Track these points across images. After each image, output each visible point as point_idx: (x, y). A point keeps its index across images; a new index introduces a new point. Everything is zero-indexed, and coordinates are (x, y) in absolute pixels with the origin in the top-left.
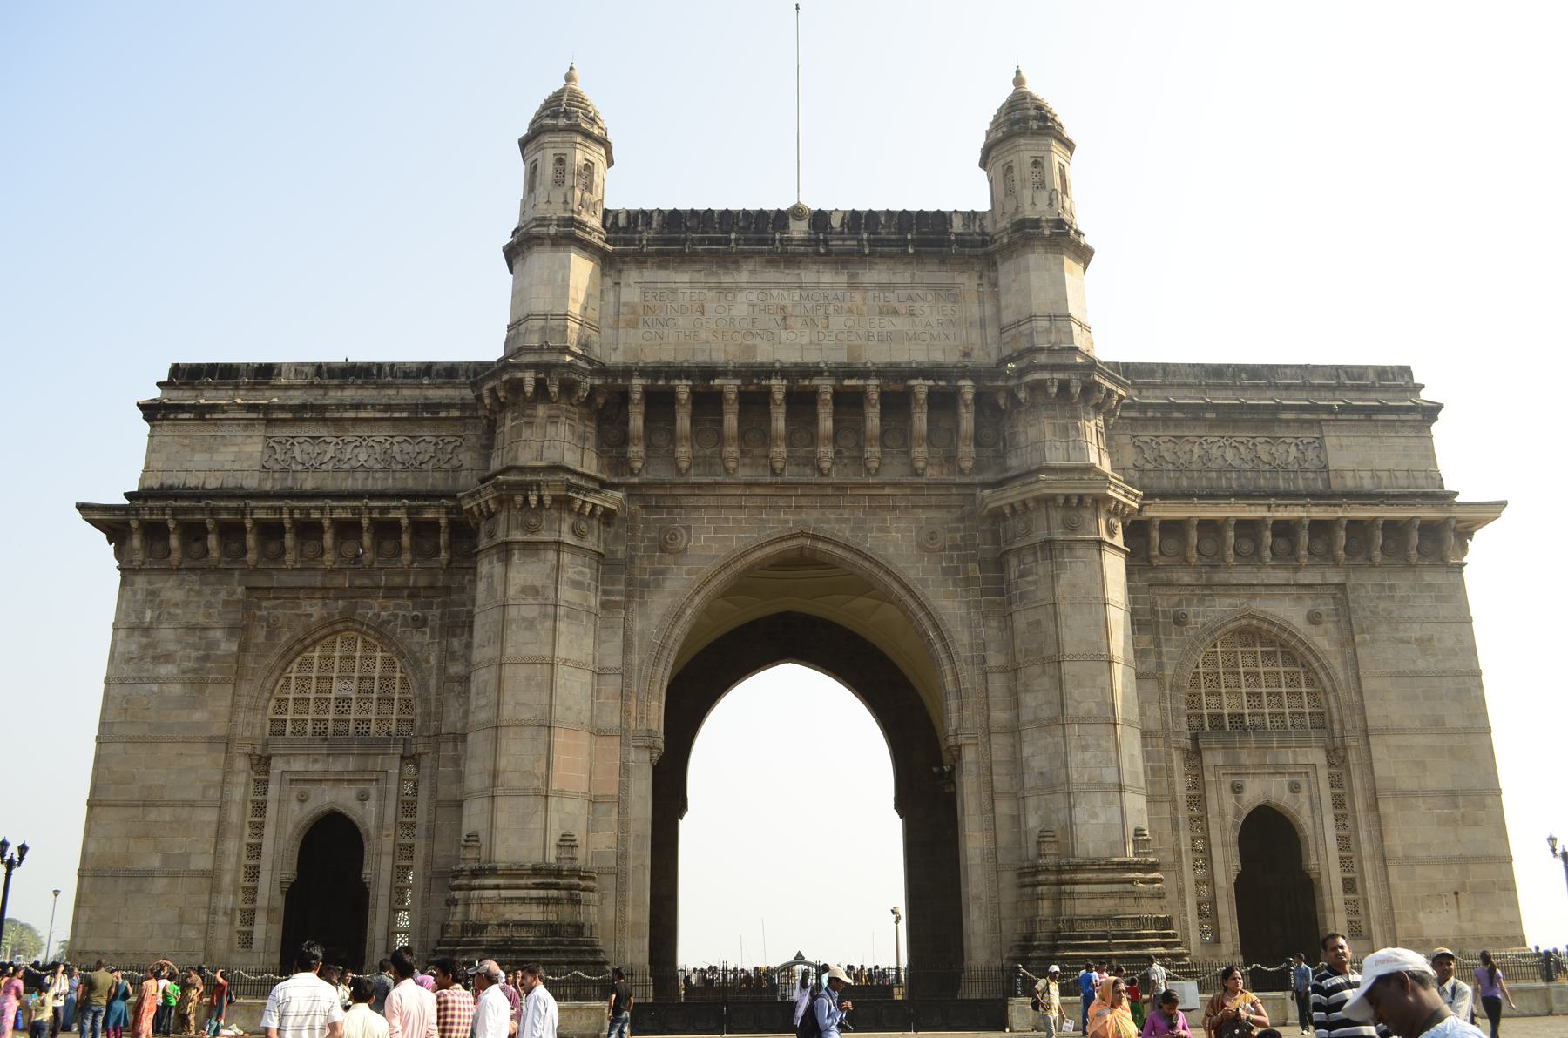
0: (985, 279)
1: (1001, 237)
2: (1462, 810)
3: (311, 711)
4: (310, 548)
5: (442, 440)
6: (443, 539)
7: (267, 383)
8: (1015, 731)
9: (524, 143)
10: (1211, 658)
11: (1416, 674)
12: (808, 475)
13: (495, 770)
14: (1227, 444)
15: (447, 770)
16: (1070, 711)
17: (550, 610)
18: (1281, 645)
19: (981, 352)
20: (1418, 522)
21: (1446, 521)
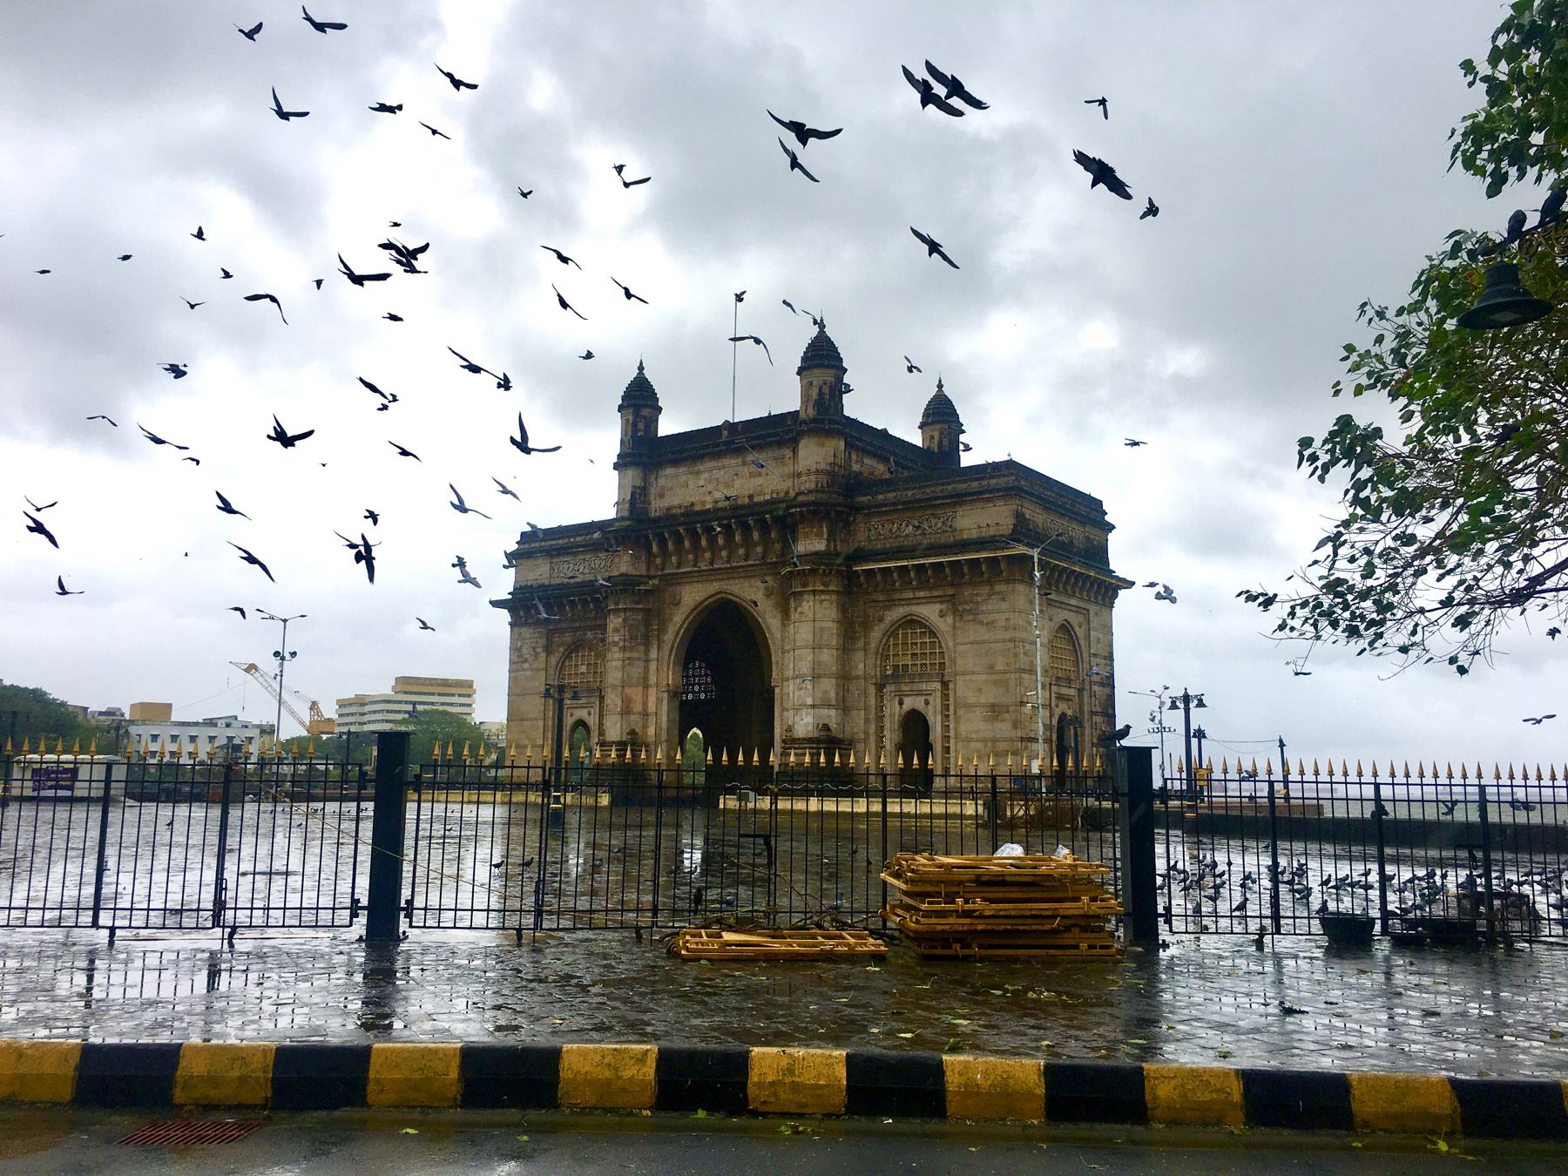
16: (796, 673)
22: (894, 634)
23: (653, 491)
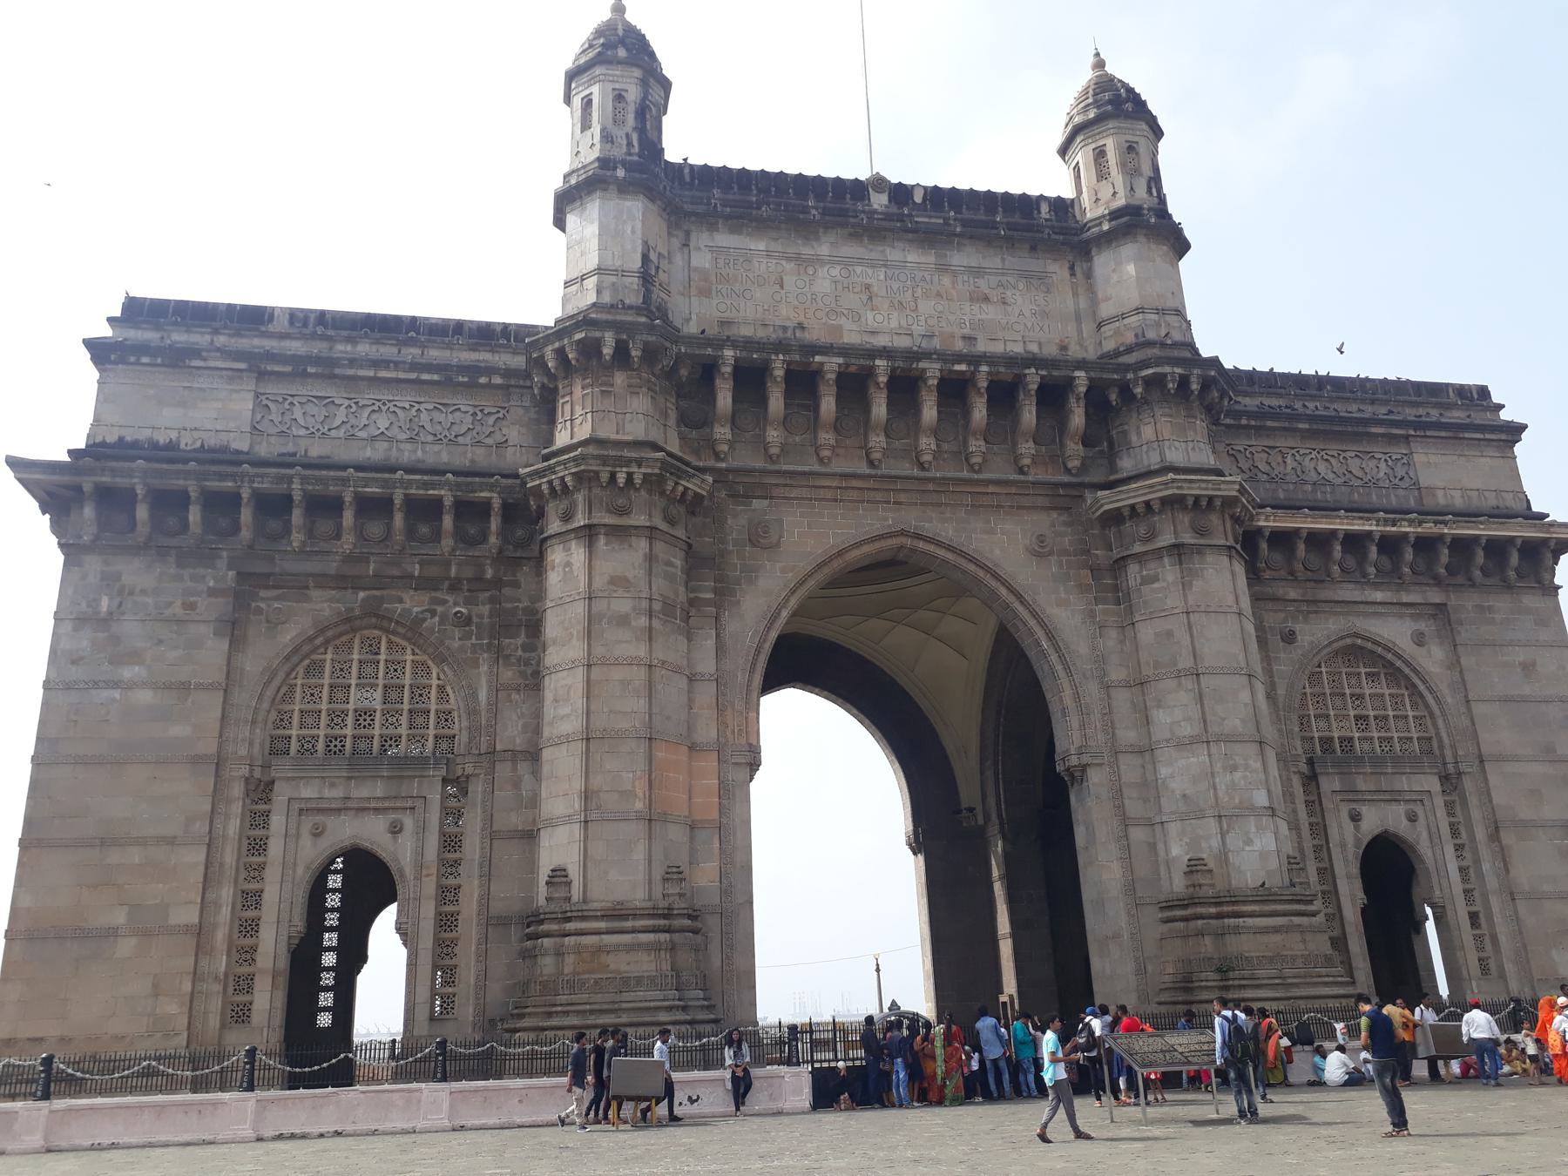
0: (1078, 269)
1: (1100, 224)
3: (323, 724)
4: (324, 526)
5: (482, 411)
6: (495, 524)
7: (257, 330)
8: (1146, 750)
9: (572, 76)
10: (1314, 677)
11: (1524, 700)
12: (906, 469)
13: (586, 792)
14: (1319, 457)
15: (503, 794)
16: (1213, 729)
17: (645, 604)
18: (1384, 666)
19: (1078, 348)
20: (1519, 542)
21: (1545, 541)
22: (1314, 677)
23: (674, 273)
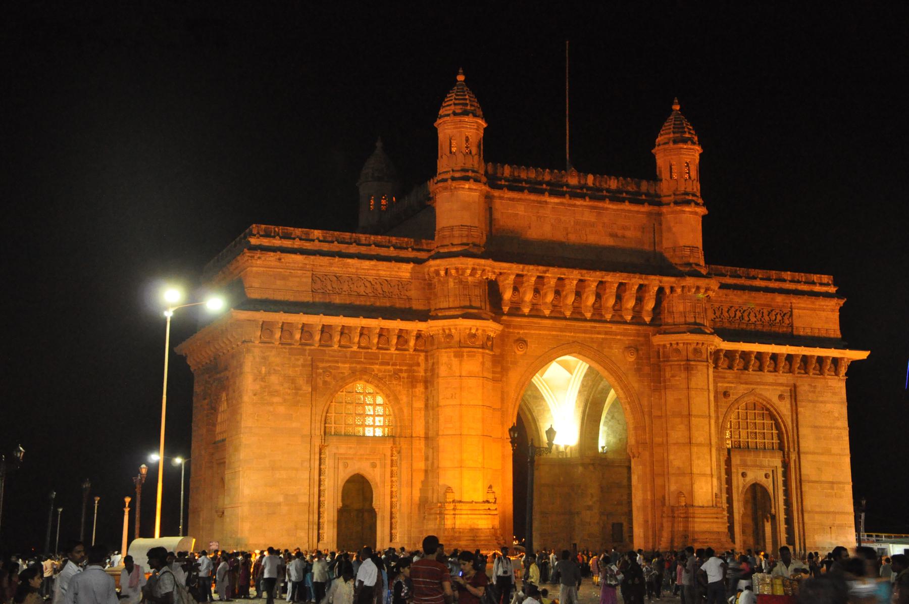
2: (835, 491)
16: (693, 441)
